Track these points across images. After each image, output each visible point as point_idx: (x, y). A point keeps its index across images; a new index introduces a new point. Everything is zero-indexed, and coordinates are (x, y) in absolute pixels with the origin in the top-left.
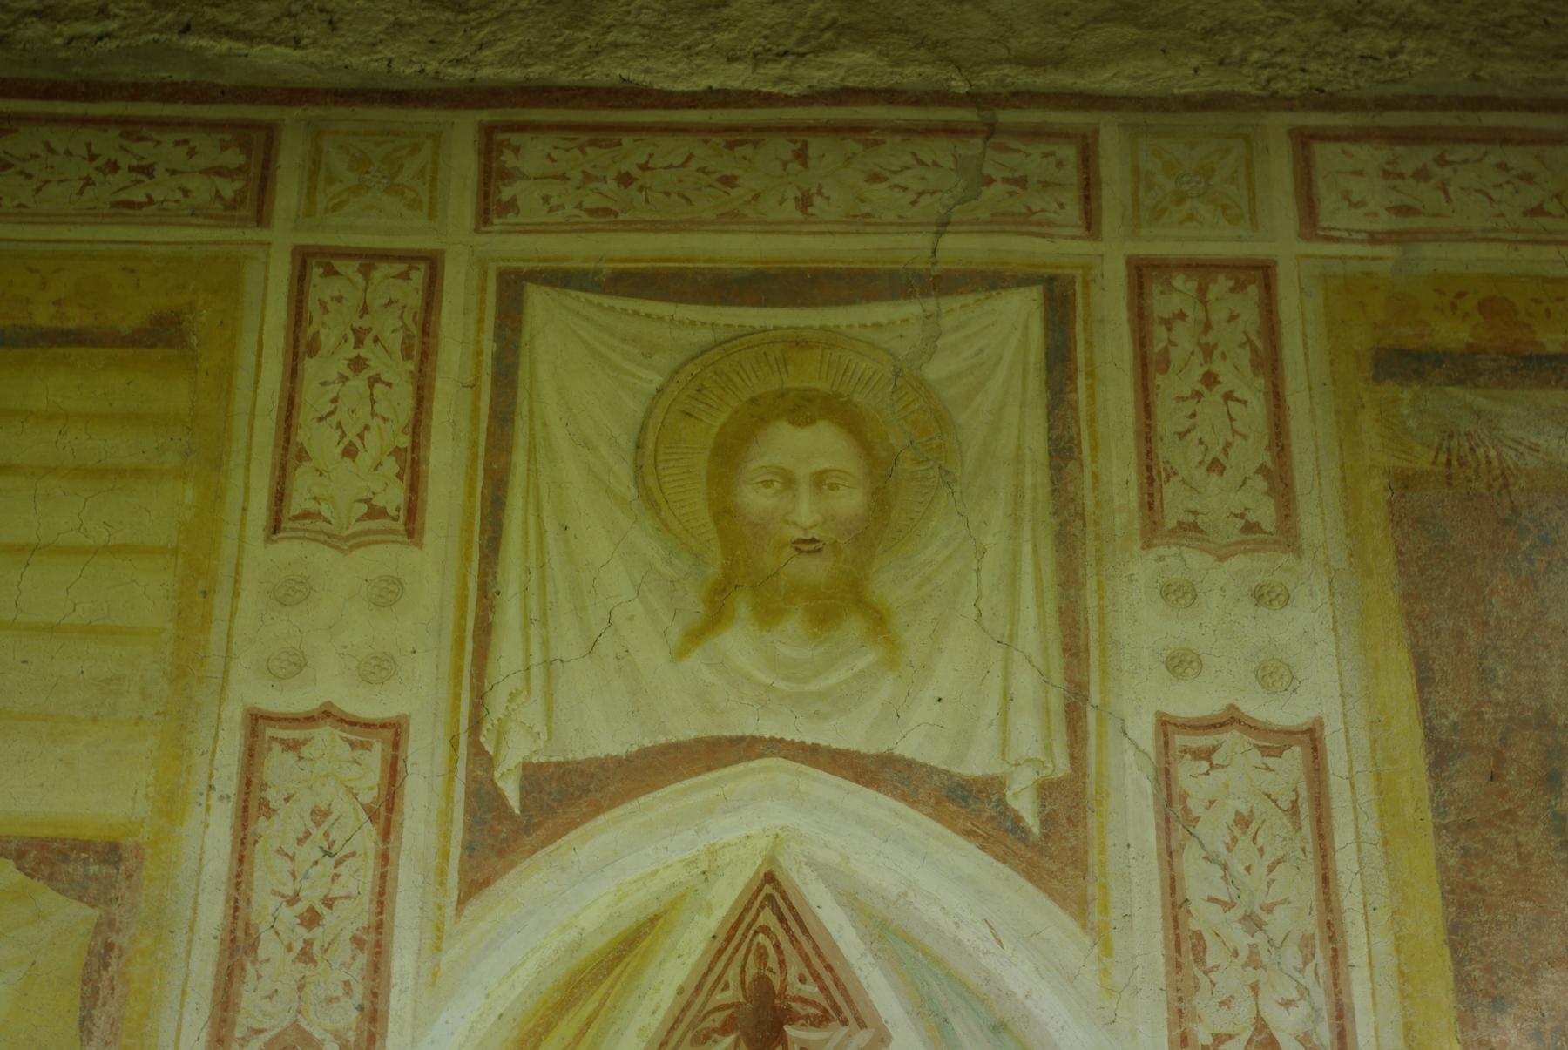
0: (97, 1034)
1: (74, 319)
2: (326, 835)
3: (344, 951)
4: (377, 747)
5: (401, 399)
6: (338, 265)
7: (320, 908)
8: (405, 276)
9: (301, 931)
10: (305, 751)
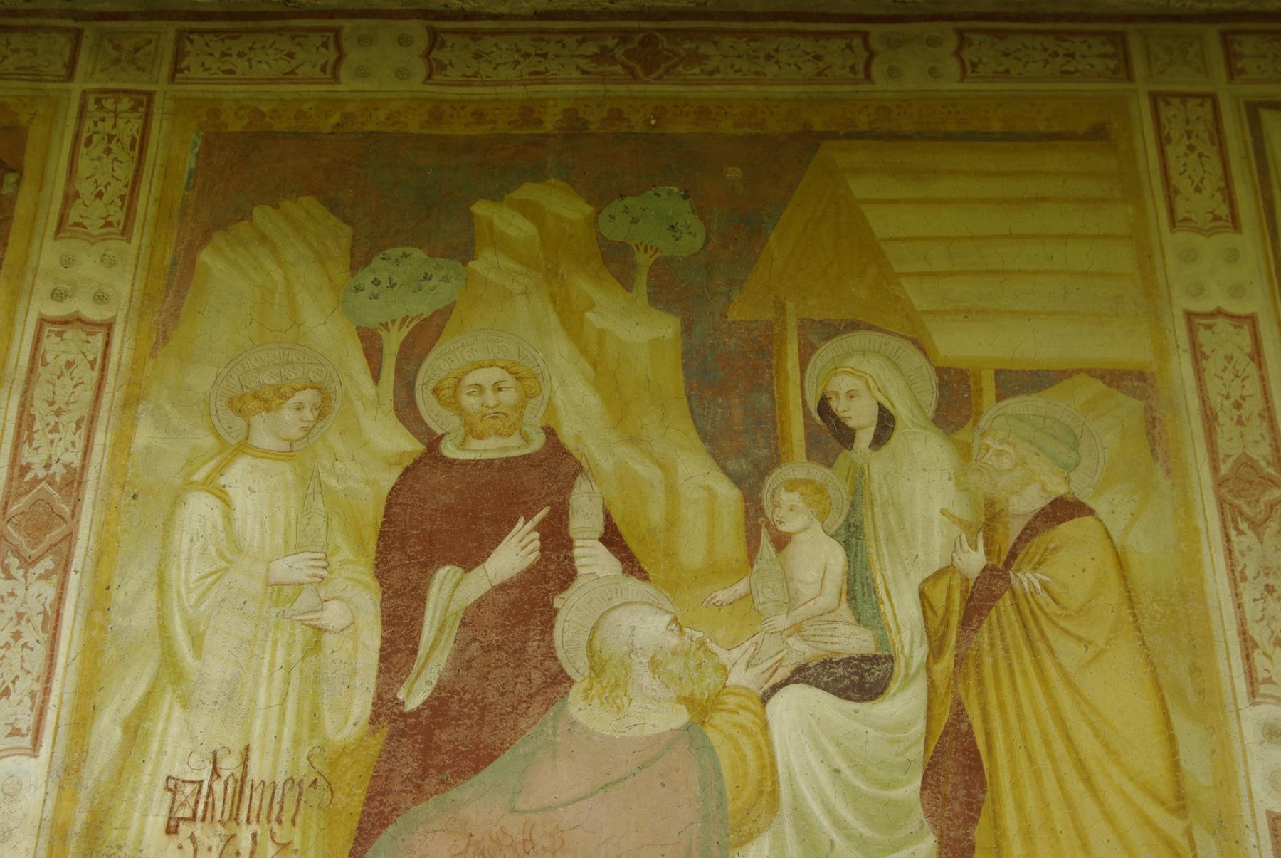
0: (1160, 457)
1: (1057, 128)
2: (1234, 367)
3: (1256, 421)
4: (1246, 327)
5: (1214, 164)
6: (1171, 100)
7: (1239, 400)
8: (1202, 105)
9: (1235, 411)
10: (1214, 329)
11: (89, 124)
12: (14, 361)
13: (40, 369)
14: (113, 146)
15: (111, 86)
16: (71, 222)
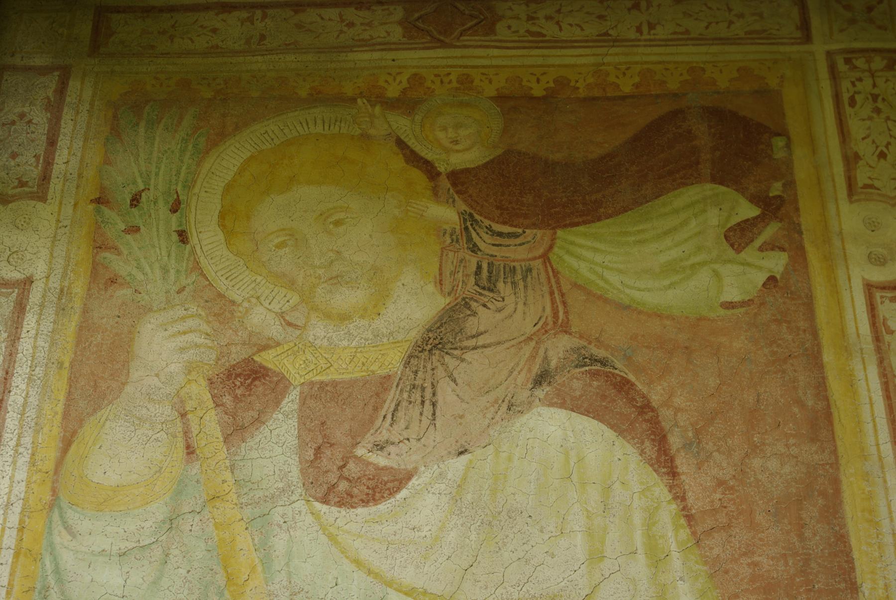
11: (845, 85)
12: (854, 329)
13: (887, 338)
14: (880, 104)
15: (857, 45)
16: (860, 184)
